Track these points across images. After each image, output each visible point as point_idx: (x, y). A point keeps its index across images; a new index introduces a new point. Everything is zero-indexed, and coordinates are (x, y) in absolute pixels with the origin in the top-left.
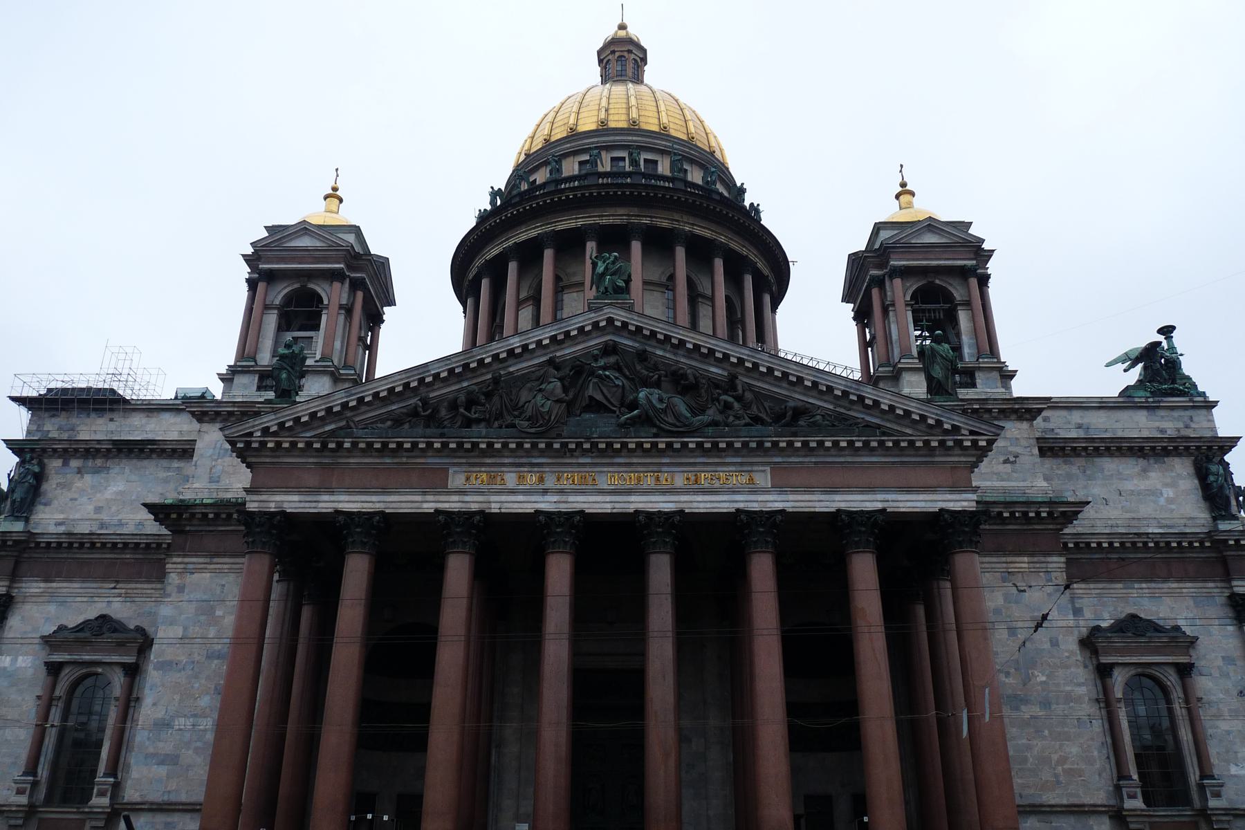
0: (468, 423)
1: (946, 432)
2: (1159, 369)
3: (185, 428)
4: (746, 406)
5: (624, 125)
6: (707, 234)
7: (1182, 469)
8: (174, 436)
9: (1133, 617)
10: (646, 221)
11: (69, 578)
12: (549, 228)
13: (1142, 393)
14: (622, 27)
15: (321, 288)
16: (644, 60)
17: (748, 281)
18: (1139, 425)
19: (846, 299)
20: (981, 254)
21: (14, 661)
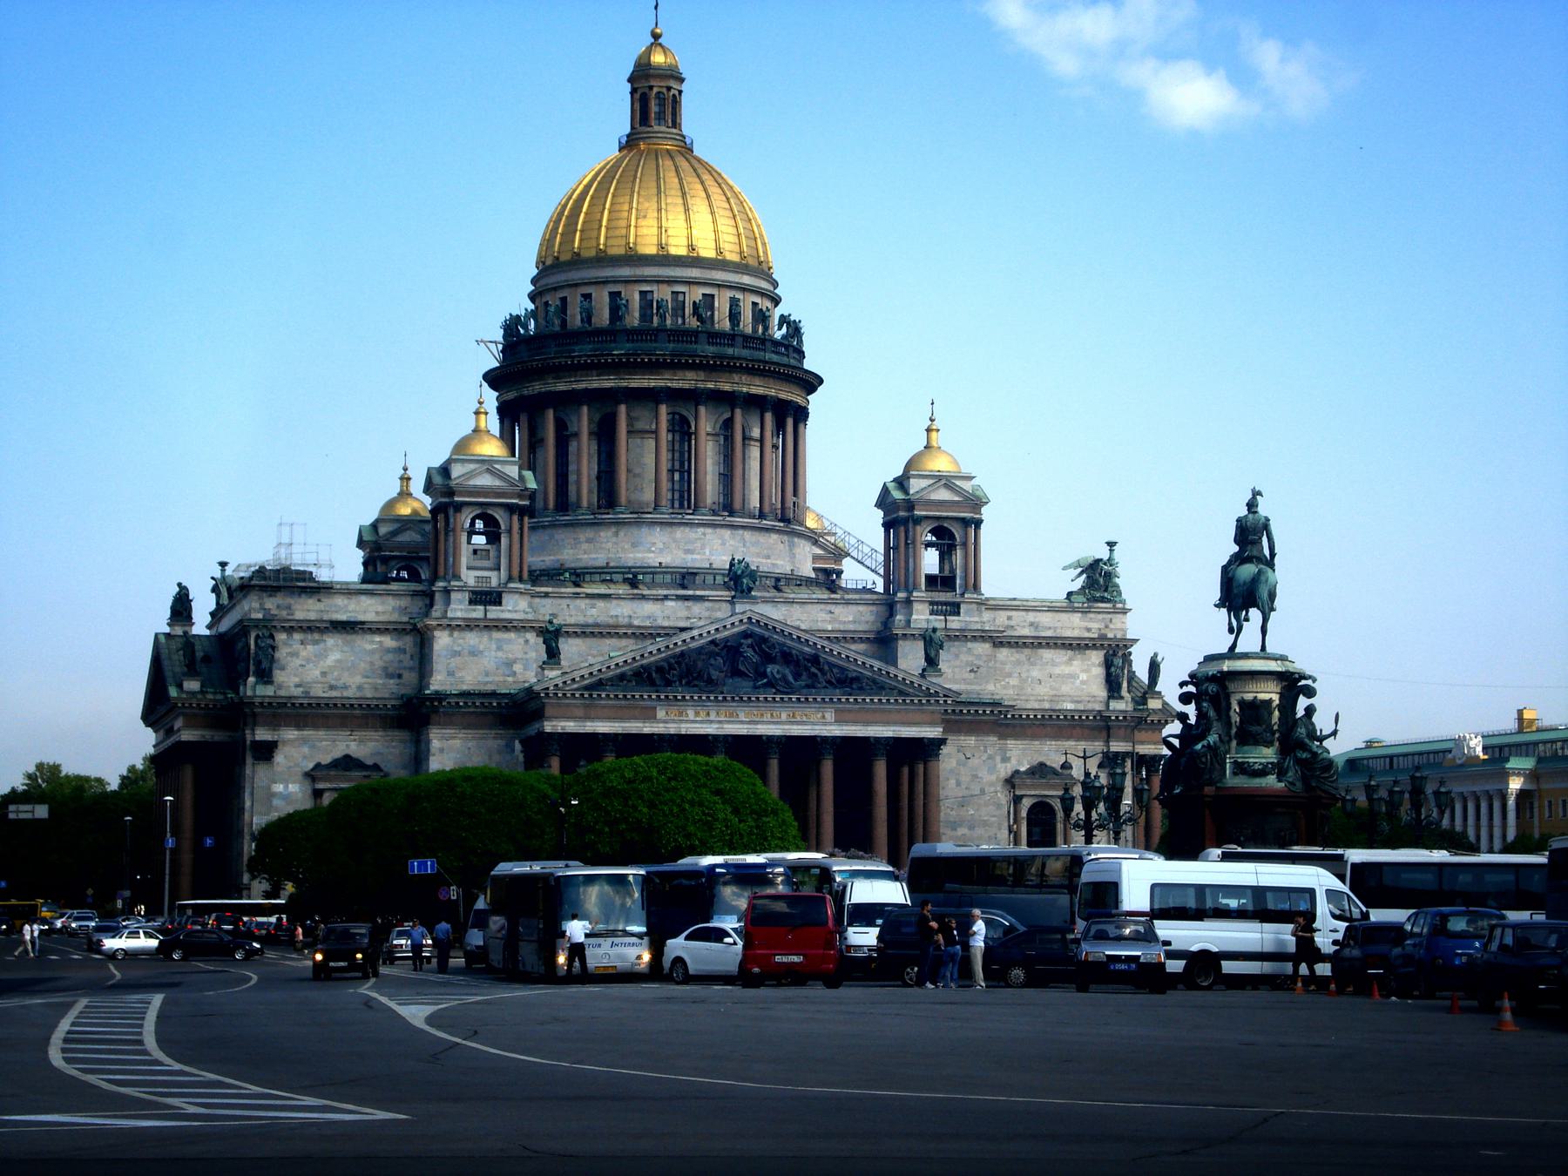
0: (668, 683)
1: (930, 695)
2: (1099, 581)
3: (380, 609)
4: (824, 674)
5: (682, 251)
6: (760, 391)
7: (1097, 657)
8: (370, 617)
9: (1042, 765)
10: (710, 385)
11: (315, 727)
12: (624, 384)
13: (1081, 598)
14: (656, 36)
15: (500, 516)
16: (680, 92)
17: (790, 422)
18: (1074, 625)
19: (879, 505)
20: (976, 502)
21: (286, 787)
